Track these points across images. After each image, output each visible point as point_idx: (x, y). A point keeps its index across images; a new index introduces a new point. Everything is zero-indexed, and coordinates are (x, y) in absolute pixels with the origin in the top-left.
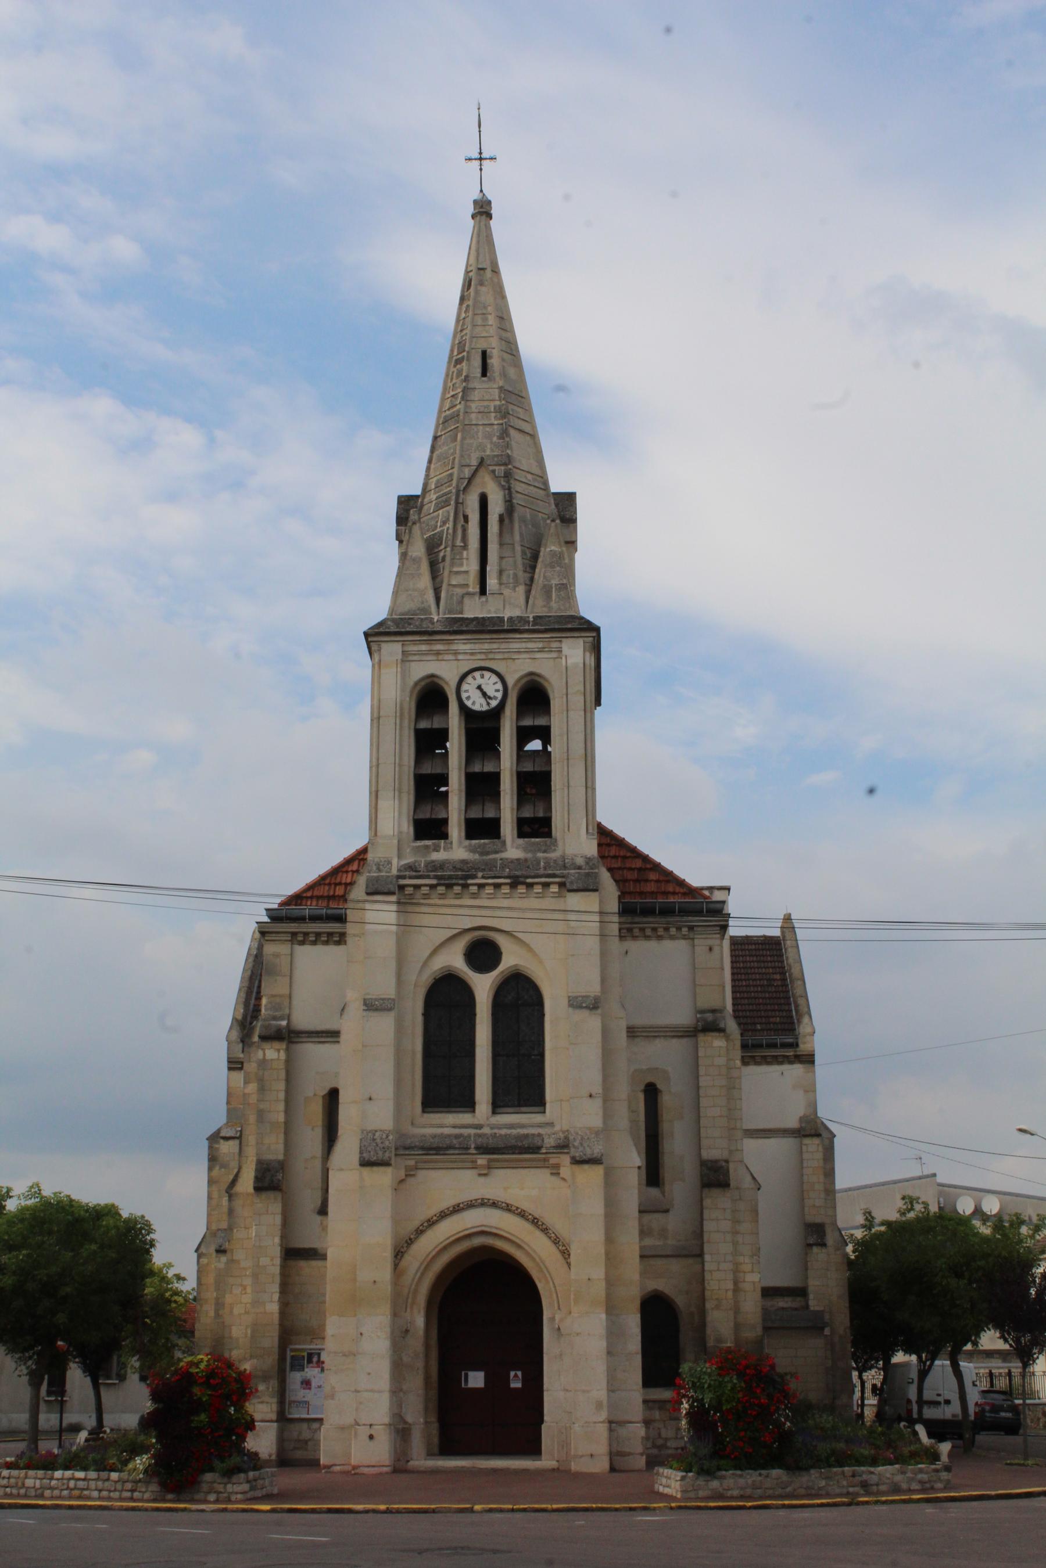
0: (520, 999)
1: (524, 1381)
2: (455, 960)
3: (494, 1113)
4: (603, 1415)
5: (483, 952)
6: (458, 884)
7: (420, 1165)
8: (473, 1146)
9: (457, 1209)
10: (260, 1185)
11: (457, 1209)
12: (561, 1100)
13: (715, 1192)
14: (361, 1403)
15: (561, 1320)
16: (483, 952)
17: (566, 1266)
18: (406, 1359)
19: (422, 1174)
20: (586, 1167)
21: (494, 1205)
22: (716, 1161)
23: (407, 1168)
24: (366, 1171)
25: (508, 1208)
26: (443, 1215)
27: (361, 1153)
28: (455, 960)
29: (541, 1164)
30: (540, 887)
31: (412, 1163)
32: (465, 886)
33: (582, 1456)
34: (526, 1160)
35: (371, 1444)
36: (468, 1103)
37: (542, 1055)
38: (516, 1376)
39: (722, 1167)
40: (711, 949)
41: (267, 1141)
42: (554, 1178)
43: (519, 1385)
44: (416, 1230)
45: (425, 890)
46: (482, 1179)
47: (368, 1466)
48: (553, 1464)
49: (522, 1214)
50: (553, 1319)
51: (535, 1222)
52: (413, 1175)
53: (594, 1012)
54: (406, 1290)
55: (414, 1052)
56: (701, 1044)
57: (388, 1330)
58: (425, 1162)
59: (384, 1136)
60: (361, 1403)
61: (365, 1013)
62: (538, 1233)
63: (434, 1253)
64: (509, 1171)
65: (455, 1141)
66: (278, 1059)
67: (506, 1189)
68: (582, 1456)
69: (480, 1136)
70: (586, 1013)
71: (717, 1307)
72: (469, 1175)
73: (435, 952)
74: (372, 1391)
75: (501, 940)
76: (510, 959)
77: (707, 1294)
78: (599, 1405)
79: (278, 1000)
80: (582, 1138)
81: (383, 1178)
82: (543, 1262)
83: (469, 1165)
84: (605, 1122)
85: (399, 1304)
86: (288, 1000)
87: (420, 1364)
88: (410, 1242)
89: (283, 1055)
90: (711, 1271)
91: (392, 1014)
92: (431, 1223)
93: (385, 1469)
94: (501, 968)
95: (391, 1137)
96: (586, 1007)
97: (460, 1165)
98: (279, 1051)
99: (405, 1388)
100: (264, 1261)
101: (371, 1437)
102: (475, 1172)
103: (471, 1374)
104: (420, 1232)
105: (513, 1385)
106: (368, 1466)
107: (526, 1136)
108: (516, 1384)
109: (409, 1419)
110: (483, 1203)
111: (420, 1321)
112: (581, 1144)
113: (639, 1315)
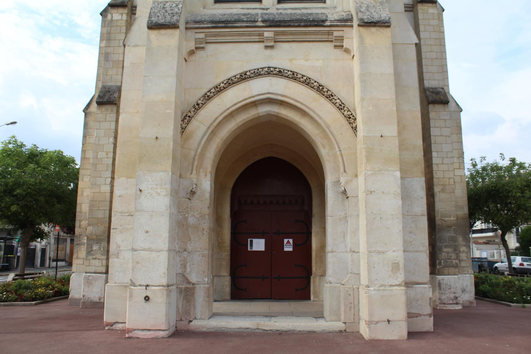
1: (295, 246)
4: (400, 278)
7: (210, 39)
8: (260, 20)
9: (244, 77)
10: (100, 100)
11: (244, 77)
13: (438, 107)
14: (138, 263)
17: (351, 131)
18: (191, 220)
19: (210, 48)
20: (373, 29)
21: (280, 73)
22: (435, 88)
23: (197, 41)
24: (154, 34)
25: (294, 77)
26: (230, 83)
27: (150, 17)
29: (325, 37)
31: (202, 36)
33: (377, 322)
34: (310, 33)
35: (147, 305)
38: (288, 242)
39: (440, 92)
41: (110, 72)
42: (338, 52)
43: (291, 249)
44: (204, 96)
46: (269, 52)
47: (143, 330)
48: (339, 326)
49: (307, 82)
50: (337, 182)
51: (320, 89)
52: (203, 48)
54: (193, 153)
56: (420, 11)
57: (168, 186)
58: (215, 35)
59: (174, 5)
60: (138, 263)
62: (323, 101)
63: (221, 118)
65: (243, 17)
66: (121, 20)
67: (291, 60)
69: (266, 14)
71: (443, 191)
74: (150, 250)
77: (435, 180)
78: (395, 267)
81: (170, 40)
82: (328, 127)
83: (256, 38)
85: (182, 165)
87: (206, 224)
88: (198, 107)
89: (125, 17)
90: (437, 164)
92: (219, 90)
93: (162, 334)
95: (180, 6)
97: (247, 38)
98: (122, 14)
99: (190, 247)
100: (101, 155)
101: (147, 299)
102: (262, 45)
103: (255, 241)
104: (207, 98)
105: (286, 249)
106: (143, 330)
107: (311, 14)
109: (193, 278)
111: (206, 185)
112: (368, 10)
113: (424, 179)
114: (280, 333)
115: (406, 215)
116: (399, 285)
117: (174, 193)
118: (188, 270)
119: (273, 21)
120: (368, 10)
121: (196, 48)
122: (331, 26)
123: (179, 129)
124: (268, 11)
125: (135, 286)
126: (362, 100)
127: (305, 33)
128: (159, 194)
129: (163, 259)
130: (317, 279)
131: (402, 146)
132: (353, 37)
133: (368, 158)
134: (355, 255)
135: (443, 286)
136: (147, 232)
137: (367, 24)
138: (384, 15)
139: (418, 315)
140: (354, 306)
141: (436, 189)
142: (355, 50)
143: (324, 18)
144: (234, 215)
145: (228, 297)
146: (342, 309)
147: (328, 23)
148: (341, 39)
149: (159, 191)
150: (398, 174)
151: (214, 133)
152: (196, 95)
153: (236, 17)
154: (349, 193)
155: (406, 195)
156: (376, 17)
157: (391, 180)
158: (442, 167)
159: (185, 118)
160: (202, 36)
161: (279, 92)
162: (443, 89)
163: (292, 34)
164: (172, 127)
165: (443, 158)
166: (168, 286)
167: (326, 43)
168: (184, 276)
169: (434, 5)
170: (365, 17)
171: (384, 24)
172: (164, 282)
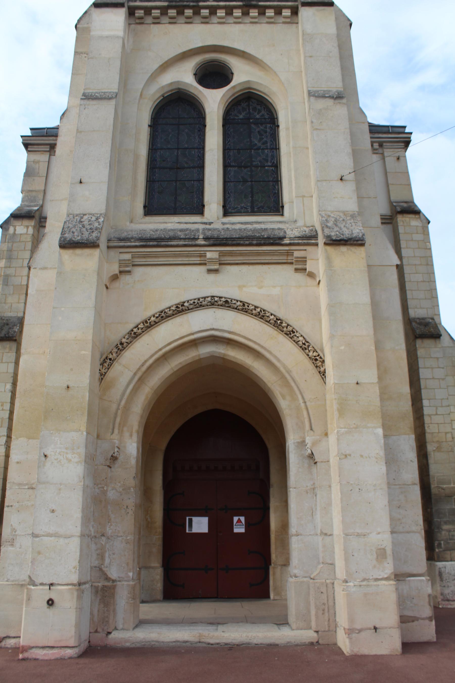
0: (253, 118)
1: (248, 525)
2: (185, 76)
3: (226, 213)
4: (388, 568)
5: (214, 74)
6: (189, 7)
7: (138, 261)
8: (201, 237)
9: (180, 309)
11: (180, 309)
12: (303, 196)
13: (428, 342)
14: (39, 553)
15: (314, 443)
16: (214, 74)
17: (318, 376)
18: (112, 495)
19: (139, 272)
20: (344, 249)
21: (227, 304)
22: (423, 319)
23: (122, 263)
24: (67, 254)
25: (244, 308)
26: (164, 316)
27: (63, 233)
28: (185, 76)
29: (283, 258)
30: (272, 11)
31: (128, 256)
32: (197, 12)
33: (360, 631)
35: (50, 612)
36: (198, 208)
37: (277, 166)
38: (239, 521)
40: (398, 159)
41: (10, 300)
42: (300, 276)
43: (242, 530)
44: (130, 333)
45: (156, 13)
46: (212, 277)
47: (43, 648)
48: (309, 635)
49: (261, 315)
50: (302, 444)
51: (278, 324)
52: (129, 272)
53: (337, 101)
54: (114, 406)
55: (137, 157)
57: (82, 451)
58: (145, 256)
59: (94, 218)
60: (39, 553)
61: (82, 102)
63: (151, 361)
64: (244, 268)
65: (179, 233)
66: (27, 234)
67: (240, 287)
68: (360, 631)
69: (209, 230)
70: (330, 102)
71: (439, 449)
72: (198, 272)
73: (165, 67)
74: (56, 535)
75: (235, 63)
76: (243, 75)
77: (428, 437)
78: (381, 554)
79: (34, 194)
80: (336, 220)
81: (88, 262)
82: (289, 372)
83: (197, 260)
84: (360, 205)
85: (101, 421)
86: (42, 194)
87: (131, 500)
88: (121, 347)
89: (31, 231)
90: (430, 416)
91: (113, 102)
92: (149, 325)
93: (69, 652)
94: (232, 84)
95: (101, 220)
96: (331, 97)
98: (27, 227)
99: (109, 531)
101: (50, 603)
102: (203, 269)
103: (195, 520)
104: (134, 335)
105: (236, 530)
106: (43, 648)
107: (266, 230)
108: (239, 529)
109: (113, 573)
110: (215, 302)
111: (132, 447)
112: (336, 225)
113: (413, 436)
114: (231, 648)
115: (393, 484)
116: (387, 579)
117: (90, 459)
118: (107, 561)
119: (217, 238)
120: (336, 225)
121: (121, 272)
122: (290, 244)
123: (98, 375)
124: (212, 226)
125: (34, 585)
126: (332, 337)
127: (258, 254)
128: (70, 461)
129: (73, 547)
130: (278, 570)
131: (385, 395)
132: (319, 258)
133: (342, 412)
134: (328, 539)
135: (445, 576)
136: (53, 511)
137: (335, 242)
138: (356, 230)
139: (414, 619)
140: (328, 608)
141: (430, 448)
142: (321, 273)
143: (281, 234)
144: (168, 486)
145: (160, 596)
146: (313, 612)
147: (286, 241)
148: (303, 260)
149: (69, 456)
150: (380, 431)
151: (141, 381)
152: (120, 332)
153: (171, 234)
154: (317, 457)
155: (391, 459)
156: (347, 234)
157: (371, 439)
158: (436, 419)
159: (104, 361)
160: (128, 256)
161: (225, 328)
162: (433, 319)
163: (241, 254)
164: (88, 374)
165: (437, 408)
166: (80, 584)
167: (285, 266)
168: (101, 569)
169: (417, 216)
170: (333, 234)
171: (356, 242)
172: (75, 578)
